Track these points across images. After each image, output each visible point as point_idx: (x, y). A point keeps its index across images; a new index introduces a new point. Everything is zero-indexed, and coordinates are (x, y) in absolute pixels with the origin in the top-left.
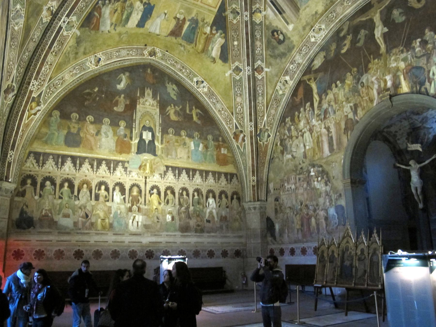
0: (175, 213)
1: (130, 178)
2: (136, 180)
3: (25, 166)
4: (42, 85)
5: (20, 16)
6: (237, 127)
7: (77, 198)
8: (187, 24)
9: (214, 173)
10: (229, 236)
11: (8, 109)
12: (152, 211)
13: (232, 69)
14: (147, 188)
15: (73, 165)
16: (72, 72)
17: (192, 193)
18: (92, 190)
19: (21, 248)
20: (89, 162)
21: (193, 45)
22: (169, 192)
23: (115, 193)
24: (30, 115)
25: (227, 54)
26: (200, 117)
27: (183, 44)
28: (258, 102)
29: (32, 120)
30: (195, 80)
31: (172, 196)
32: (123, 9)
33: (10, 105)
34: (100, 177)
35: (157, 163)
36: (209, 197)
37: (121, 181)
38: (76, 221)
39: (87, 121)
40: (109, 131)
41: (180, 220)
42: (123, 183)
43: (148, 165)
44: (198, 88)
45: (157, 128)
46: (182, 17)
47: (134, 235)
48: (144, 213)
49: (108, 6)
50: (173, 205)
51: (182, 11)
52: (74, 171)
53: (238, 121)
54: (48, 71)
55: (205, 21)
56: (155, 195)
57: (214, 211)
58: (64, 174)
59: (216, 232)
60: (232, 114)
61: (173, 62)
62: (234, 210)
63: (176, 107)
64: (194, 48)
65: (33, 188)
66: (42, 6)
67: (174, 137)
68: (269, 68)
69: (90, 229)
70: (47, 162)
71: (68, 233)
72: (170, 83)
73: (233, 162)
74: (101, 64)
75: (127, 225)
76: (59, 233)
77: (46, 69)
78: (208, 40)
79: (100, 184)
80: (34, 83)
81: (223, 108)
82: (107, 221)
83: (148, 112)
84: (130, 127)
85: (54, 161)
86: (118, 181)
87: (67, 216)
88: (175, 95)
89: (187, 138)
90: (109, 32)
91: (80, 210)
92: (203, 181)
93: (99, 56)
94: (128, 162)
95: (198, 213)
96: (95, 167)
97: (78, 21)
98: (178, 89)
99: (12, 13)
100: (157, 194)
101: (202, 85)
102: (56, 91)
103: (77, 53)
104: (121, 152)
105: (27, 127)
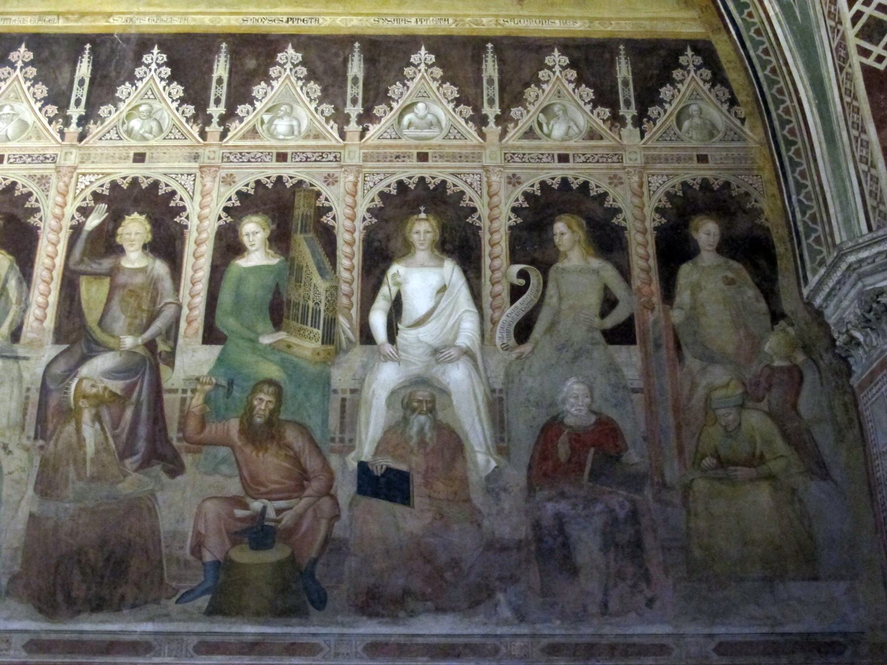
17: (211, 227)
36: (408, 249)
62: (709, 358)
92: (341, 119)
95: (263, 402)
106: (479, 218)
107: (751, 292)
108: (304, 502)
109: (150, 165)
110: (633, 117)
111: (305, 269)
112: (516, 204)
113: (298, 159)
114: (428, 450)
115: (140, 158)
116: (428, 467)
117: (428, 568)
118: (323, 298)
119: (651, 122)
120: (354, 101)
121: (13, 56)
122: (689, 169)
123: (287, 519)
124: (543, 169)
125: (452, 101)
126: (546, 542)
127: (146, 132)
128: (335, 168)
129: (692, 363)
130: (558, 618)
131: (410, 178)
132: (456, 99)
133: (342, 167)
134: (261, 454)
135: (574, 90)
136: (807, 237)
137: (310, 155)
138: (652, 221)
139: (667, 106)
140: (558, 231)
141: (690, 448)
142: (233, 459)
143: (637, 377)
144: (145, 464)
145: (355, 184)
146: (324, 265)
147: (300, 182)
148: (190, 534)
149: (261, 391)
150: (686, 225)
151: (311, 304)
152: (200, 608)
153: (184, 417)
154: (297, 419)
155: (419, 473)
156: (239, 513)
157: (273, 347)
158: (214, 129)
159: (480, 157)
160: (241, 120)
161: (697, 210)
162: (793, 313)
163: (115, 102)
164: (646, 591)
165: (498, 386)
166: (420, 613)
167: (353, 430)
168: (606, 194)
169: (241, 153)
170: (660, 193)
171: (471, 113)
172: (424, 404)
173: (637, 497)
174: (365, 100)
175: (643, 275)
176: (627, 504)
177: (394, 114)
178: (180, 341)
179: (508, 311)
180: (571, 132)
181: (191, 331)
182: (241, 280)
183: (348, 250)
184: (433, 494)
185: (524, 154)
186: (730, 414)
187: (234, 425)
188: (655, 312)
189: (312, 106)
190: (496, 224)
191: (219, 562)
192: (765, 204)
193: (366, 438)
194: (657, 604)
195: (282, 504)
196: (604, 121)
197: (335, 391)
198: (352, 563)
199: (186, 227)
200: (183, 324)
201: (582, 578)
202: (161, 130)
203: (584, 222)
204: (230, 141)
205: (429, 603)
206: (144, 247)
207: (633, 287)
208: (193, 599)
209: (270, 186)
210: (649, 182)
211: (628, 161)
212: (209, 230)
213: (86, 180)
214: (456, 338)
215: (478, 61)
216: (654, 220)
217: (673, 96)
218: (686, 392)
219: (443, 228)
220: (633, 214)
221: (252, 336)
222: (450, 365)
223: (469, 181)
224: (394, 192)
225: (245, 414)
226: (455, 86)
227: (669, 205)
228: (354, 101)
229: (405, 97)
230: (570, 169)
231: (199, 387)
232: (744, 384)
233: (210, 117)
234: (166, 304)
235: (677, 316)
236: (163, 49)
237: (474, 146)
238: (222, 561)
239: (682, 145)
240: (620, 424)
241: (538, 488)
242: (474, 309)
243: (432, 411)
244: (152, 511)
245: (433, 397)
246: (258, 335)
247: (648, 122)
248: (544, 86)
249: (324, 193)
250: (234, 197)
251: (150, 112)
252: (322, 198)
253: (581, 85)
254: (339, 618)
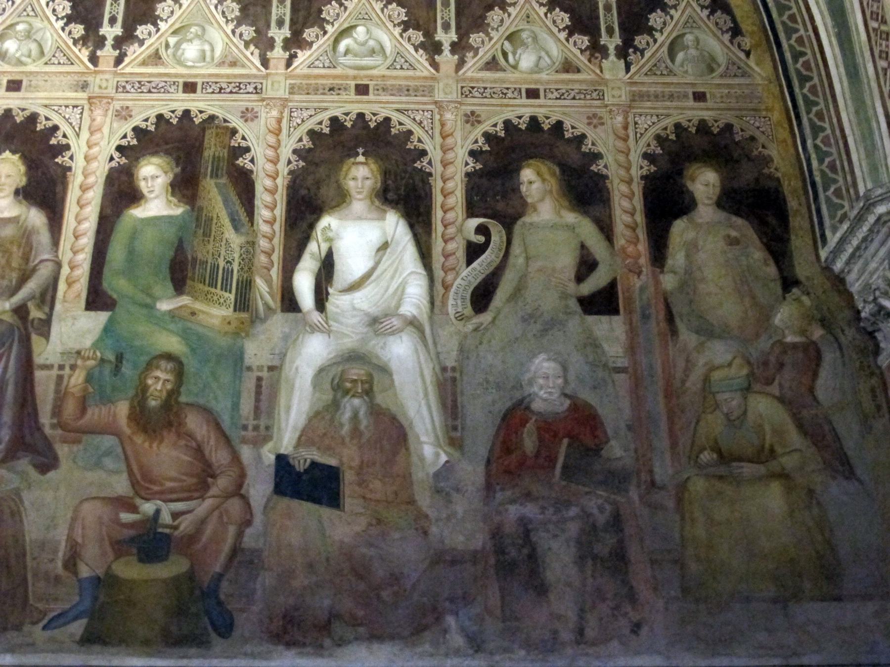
17: (101, 169)
36: (342, 199)
92: (264, 43)
106: (430, 163)
107: (758, 254)
108: (208, 503)
109: (29, 95)
110: (617, 48)
111: (215, 221)
112: (475, 147)
113: (210, 90)
114: (364, 440)
115: (14, 86)
116: (362, 462)
117: (362, 586)
118: (236, 256)
119: (639, 53)
120: (280, 23)
122: (684, 109)
123: (186, 524)
124: (507, 106)
125: (399, 24)
126: (508, 554)
127: (22, 55)
128: (254, 101)
129: (687, 337)
130: (521, 647)
131: (347, 114)
132: (403, 22)
133: (263, 100)
134: (155, 445)
135: (546, 14)
136: (825, 190)
137: (224, 86)
138: (639, 168)
139: (657, 35)
140: (525, 179)
141: (684, 440)
142: (119, 450)
143: (621, 354)
145: (279, 121)
146: (238, 216)
147: (212, 118)
148: (63, 544)
149: (158, 367)
150: (680, 173)
151: (222, 264)
152: (72, 635)
154: (201, 401)
155: (351, 468)
156: (126, 517)
157: (172, 315)
158: (108, 53)
159: (431, 90)
160: (141, 42)
161: (693, 158)
162: (808, 278)
164: (631, 614)
165: (450, 363)
166: (350, 642)
167: (270, 414)
168: (583, 136)
169: (139, 82)
170: (649, 136)
171: (422, 39)
172: (360, 384)
173: (619, 498)
174: (293, 22)
175: (628, 233)
176: (608, 507)
177: (329, 39)
178: (58, 307)
179: (464, 274)
180: (542, 64)
181: (71, 295)
182: (134, 235)
183: (268, 198)
184: (368, 496)
185: (485, 88)
186: (733, 399)
187: (122, 409)
188: (643, 277)
189: (229, 28)
190: (450, 170)
191: (99, 578)
192: (773, 151)
193: (287, 425)
194: (645, 630)
195: (179, 506)
196: (582, 51)
197: (249, 369)
198: (266, 579)
199: (69, 169)
200: (62, 286)
201: (552, 597)
202: (42, 53)
203: (557, 170)
204: (129, 67)
205: (361, 630)
206: (17, 192)
207: (616, 248)
208: (65, 624)
209: (174, 121)
210: (636, 123)
211: (611, 99)
212: (98, 174)
214: (398, 306)
216: (642, 168)
217: (665, 23)
218: (679, 374)
219: (386, 174)
220: (616, 160)
221: (148, 300)
222: (391, 338)
223: (417, 118)
224: (327, 131)
225: (136, 395)
226: (403, 7)
227: (659, 151)
228: (280, 23)
229: (341, 20)
230: (540, 106)
231: (79, 362)
232: (749, 363)
233: (104, 38)
234: (42, 261)
235: (669, 281)
237: (425, 78)
238: (102, 577)
239: (675, 80)
240: (600, 411)
241: (498, 488)
242: (421, 270)
243: (368, 392)
244: (16, 515)
245: (371, 376)
246: (155, 299)
247: (635, 53)
248: (510, 9)
249: (241, 131)
250: (130, 134)
251: (29, 32)
252: (238, 137)
253: (554, 9)
254: (248, 648)
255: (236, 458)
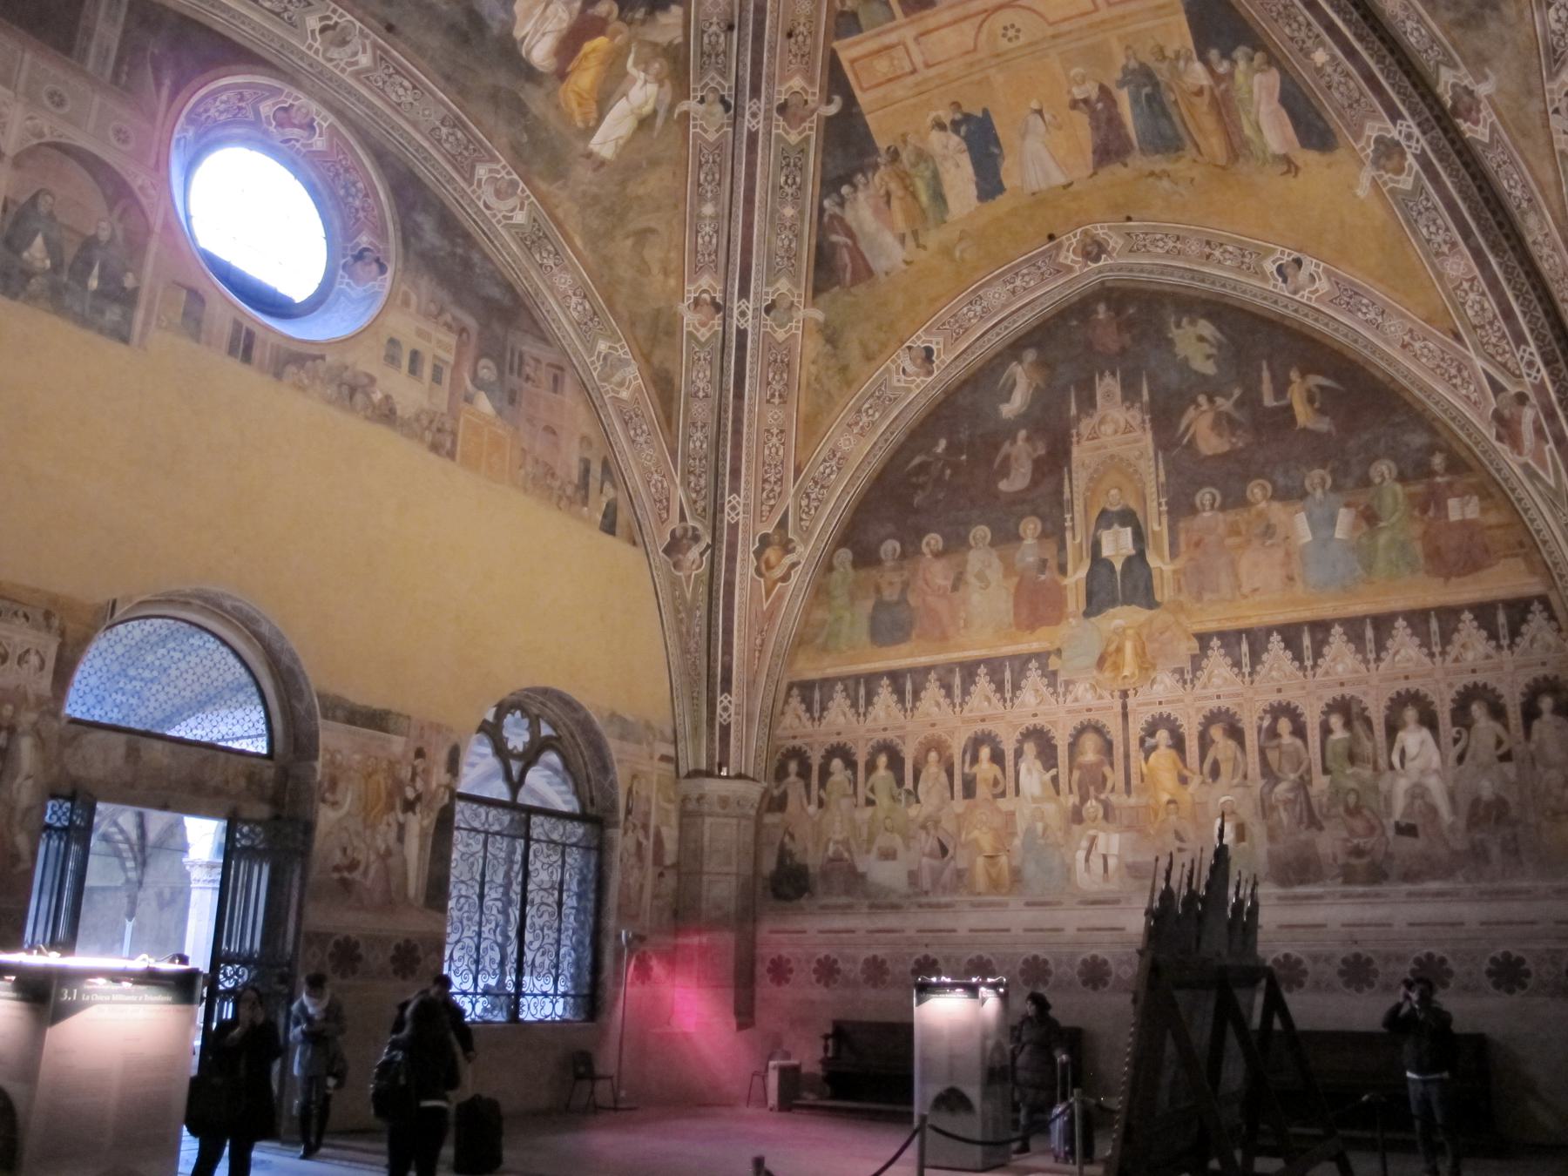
0: (1247, 812)
1: (1069, 704)
2: (1089, 710)
3: (782, 725)
4: (780, 493)
5: (623, 363)
6: (1497, 388)
7: (912, 799)
8: (1124, 98)
9: (1417, 619)
10: (1528, 892)
11: (703, 589)
12: (1156, 815)
13: (1368, 163)
14: (1131, 731)
15: (895, 697)
16: (857, 423)
18: (952, 764)
19: (785, 952)
20: (939, 680)
21: (1190, 151)
22: (1216, 732)
23: (1023, 767)
24: (769, 583)
25: (1319, 116)
26: (1323, 402)
27: (1157, 169)
28: (1534, 243)
29: (780, 597)
30: (1270, 267)
31: (1232, 744)
32: (904, 179)
33: (705, 578)
34: (973, 721)
35: (1161, 634)
36: (1404, 726)
37: (1039, 721)
38: (915, 867)
39: (923, 554)
40: (990, 566)
41: (1272, 838)
42: (1048, 727)
43: (1129, 647)
44: (1295, 292)
45: (1152, 505)
46: (1092, 91)
47: (1094, 903)
48: (1126, 822)
49: (855, 199)
50: (1236, 781)
51: (1077, 71)
52: (901, 715)
53: (1490, 358)
54: (781, 452)
55: (1169, 53)
56: (1162, 750)
57: (1434, 784)
58: (875, 730)
59: (1449, 873)
60: (1457, 337)
61: (1171, 244)
63: (1219, 400)
64: (1199, 159)
65: (801, 784)
66: (671, 307)
67: (1221, 516)
68: (1486, 78)
69: (955, 890)
70: (830, 704)
71: (895, 907)
72: (1185, 321)
73: (1521, 544)
74: (943, 362)
75: (1069, 870)
76: (871, 906)
77: (773, 450)
78: (1224, 107)
79: (977, 742)
80: (734, 502)
81: (1411, 331)
82: (1003, 860)
83: (1112, 457)
84: (1055, 532)
85: (848, 696)
86: (1031, 722)
87: (888, 855)
88: (1209, 357)
89: (1276, 506)
90: (907, 263)
91: (923, 834)
92: (1366, 661)
93: (919, 343)
94: (1059, 652)
95: (1352, 799)
96: (957, 691)
97: (797, 285)
98: (1220, 329)
99: (595, 369)
100: (1169, 747)
101: (1303, 275)
102: (831, 494)
103: (844, 369)
104: (1032, 627)
105: (770, 618)
115: (1279, 691)
121: (1212, 644)
123: (1369, 846)
129: (1540, 768)
138: (1519, 699)
144: (1308, 828)
153: (1321, 807)
156: (1349, 844)
157: (1353, 775)
158: (1310, 673)
163: (1262, 663)
187: (1341, 809)
204: (1318, 678)
213: (1258, 704)
215: (1427, 621)
235: (1532, 746)
236: (1279, 632)
243: (1423, 797)
255: (1381, 823)
